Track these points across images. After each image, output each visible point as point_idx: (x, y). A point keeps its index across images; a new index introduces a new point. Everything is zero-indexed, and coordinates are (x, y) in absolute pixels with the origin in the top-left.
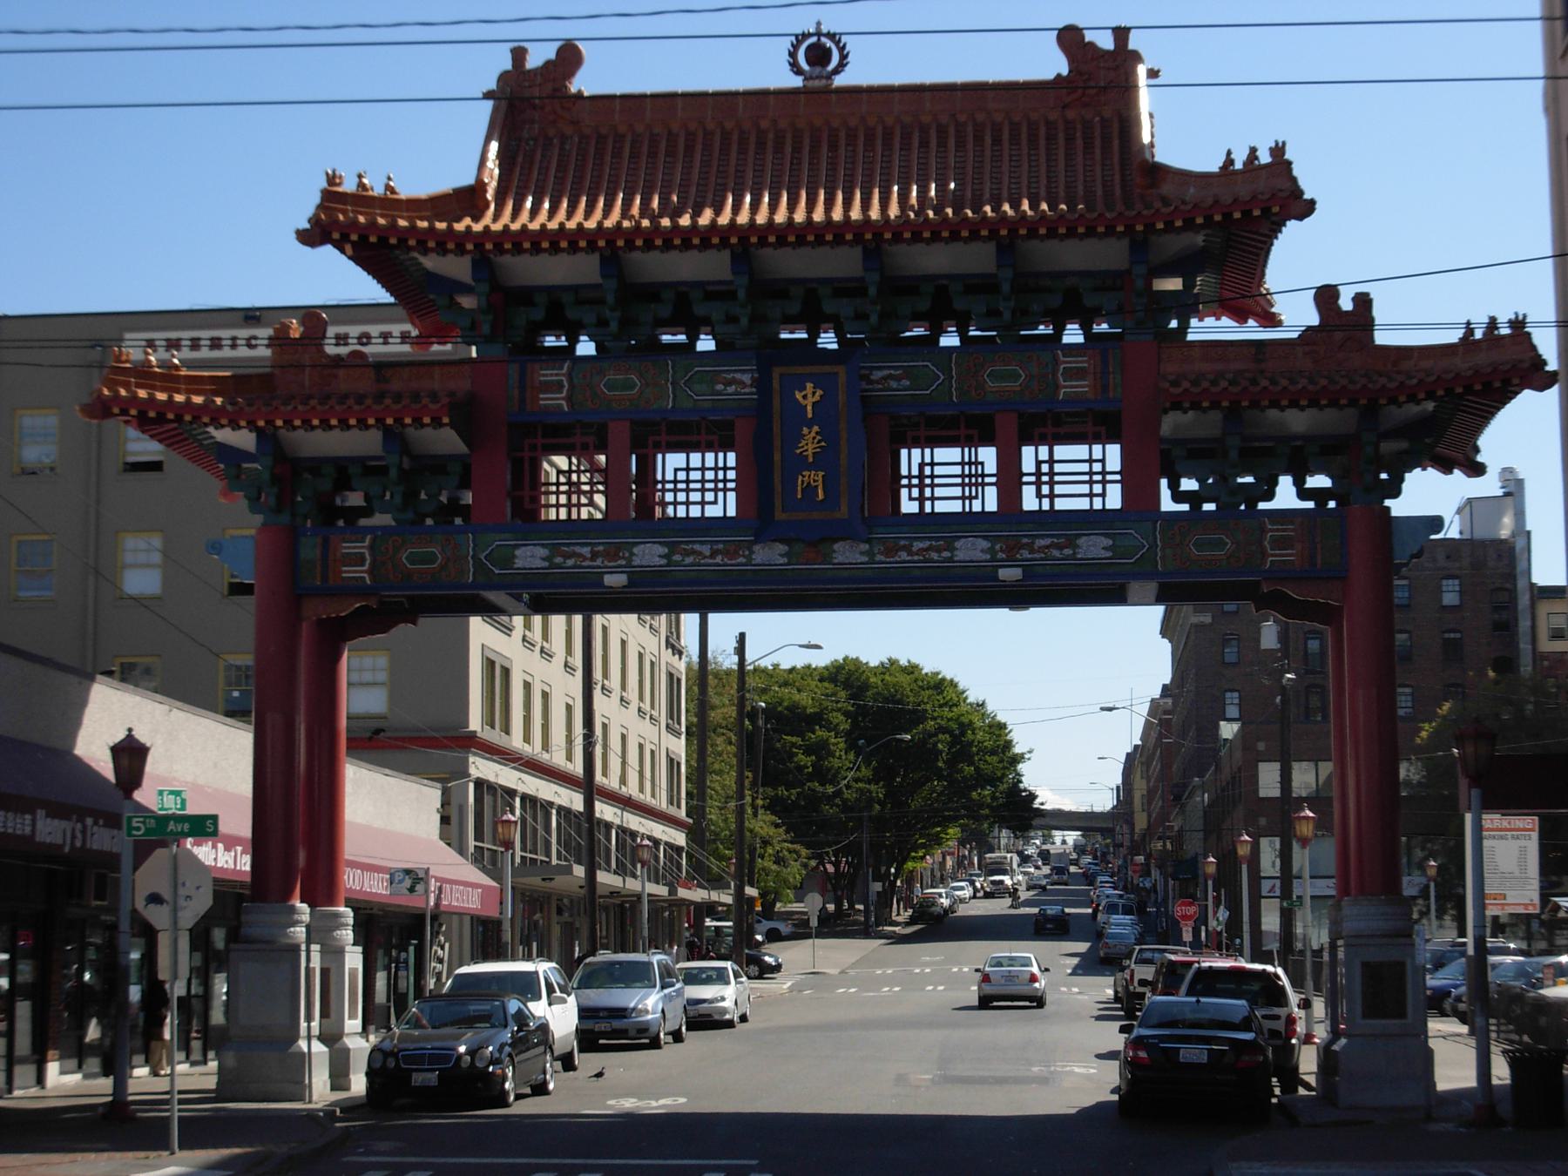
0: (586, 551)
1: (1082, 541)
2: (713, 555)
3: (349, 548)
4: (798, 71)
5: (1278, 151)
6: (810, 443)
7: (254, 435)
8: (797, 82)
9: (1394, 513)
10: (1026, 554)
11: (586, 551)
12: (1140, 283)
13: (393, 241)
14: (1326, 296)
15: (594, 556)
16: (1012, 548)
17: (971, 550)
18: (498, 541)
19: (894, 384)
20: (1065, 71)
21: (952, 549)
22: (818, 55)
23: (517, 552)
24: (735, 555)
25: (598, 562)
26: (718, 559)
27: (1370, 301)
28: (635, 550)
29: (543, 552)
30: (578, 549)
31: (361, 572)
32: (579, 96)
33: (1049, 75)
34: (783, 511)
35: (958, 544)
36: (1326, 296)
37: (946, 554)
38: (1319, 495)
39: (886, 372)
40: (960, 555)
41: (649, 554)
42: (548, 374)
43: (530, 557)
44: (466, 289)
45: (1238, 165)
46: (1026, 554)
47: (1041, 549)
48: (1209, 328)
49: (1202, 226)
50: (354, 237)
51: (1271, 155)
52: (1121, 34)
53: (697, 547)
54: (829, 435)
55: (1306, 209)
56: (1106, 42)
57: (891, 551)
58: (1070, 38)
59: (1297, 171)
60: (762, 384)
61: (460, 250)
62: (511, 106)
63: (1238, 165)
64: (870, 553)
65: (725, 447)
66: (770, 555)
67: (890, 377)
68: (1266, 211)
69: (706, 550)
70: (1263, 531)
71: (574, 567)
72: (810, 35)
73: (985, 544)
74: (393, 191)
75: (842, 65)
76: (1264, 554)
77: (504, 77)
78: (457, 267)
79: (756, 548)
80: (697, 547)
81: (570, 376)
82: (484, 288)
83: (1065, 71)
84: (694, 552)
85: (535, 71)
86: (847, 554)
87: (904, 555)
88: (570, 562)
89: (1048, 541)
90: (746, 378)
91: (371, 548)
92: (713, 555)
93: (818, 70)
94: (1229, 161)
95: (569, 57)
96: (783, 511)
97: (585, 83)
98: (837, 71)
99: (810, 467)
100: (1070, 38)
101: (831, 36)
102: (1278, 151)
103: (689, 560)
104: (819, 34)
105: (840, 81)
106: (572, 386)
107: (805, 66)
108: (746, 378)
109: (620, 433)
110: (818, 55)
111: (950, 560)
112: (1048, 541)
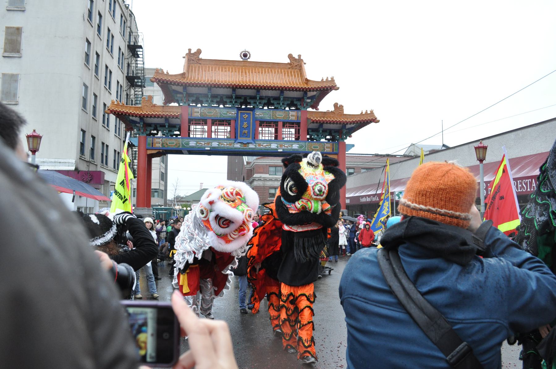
0: (203, 143)
1: (293, 145)
2: (227, 144)
3: (157, 140)
4: (242, 58)
5: (332, 79)
6: (245, 125)
7: (139, 119)
8: (241, 60)
9: (346, 143)
10: (283, 147)
11: (203, 143)
12: (305, 100)
13: (169, 83)
14: (336, 105)
15: (205, 144)
16: (281, 146)
17: (274, 146)
18: (186, 140)
19: (260, 115)
20: (289, 62)
21: (270, 145)
22: (245, 55)
23: (190, 142)
24: (231, 145)
25: (206, 145)
26: (228, 146)
27: (343, 106)
28: (213, 143)
29: (195, 143)
30: (202, 143)
31: (159, 145)
32: (201, 59)
33: (287, 63)
34: (240, 137)
35: (272, 145)
36: (336, 105)
37: (269, 147)
38: (328, 140)
39: (259, 113)
40: (272, 147)
41: (215, 144)
42: (196, 110)
43: (192, 144)
44: (180, 93)
45: (324, 80)
46: (283, 147)
47: (286, 147)
48: (310, 109)
49: (318, 91)
50: (161, 81)
51: (331, 79)
52: (300, 56)
53: (224, 143)
54: (249, 124)
55: (338, 89)
56: (297, 57)
57: (259, 145)
58: (290, 56)
59: (336, 81)
60: (237, 114)
61: (182, 85)
62: (188, 60)
63: (324, 80)
64: (255, 146)
65: (229, 124)
66: (238, 146)
67: (259, 114)
68: (331, 88)
69: (225, 144)
70: (325, 145)
71: (201, 146)
72: (244, 51)
73: (276, 145)
74: (168, 73)
75: (250, 57)
76: (325, 149)
77: (187, 54)
78: (180, 89)
79: (235, 144)
80: (224, 143)
81: (200, 110)
82: (185, 93)
83: (289, 62)
84: (223, 144)
85: (193, 54)
86: (251, 146)
87: (262, 146)
88: (200, 145)
89: (287, 145)
90: (233, 113)
91: (162, 140)
92: (227, 144)
93: (245, 58)
94: (323, 80)
95: (199, 52)
96: (240, 137)
97: (202, 56)
98: (249, 58)
99: (245, 129)
100: (290, 56)
101: (248, 52)
102: (332, 79)
103: (222, 145)
104: (245, 51)
105: (249, 60)
106: (201, 113)
107: (243, 57)
108: (233, 113)
109: (209, 122)
110: (245, 55)
111: (269, 147)
112: (287, 145)
